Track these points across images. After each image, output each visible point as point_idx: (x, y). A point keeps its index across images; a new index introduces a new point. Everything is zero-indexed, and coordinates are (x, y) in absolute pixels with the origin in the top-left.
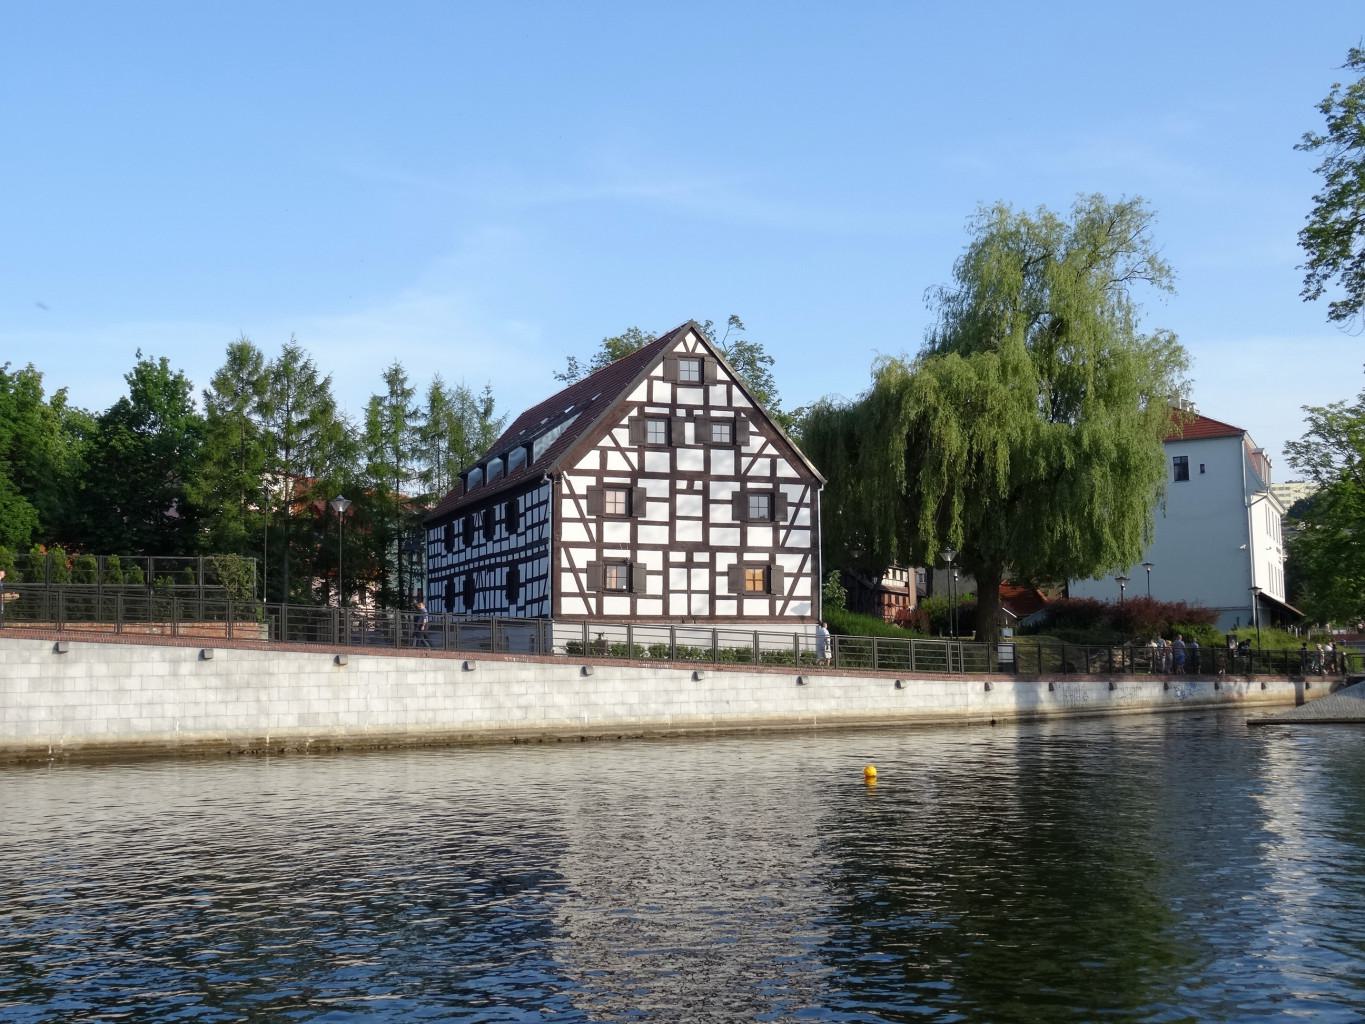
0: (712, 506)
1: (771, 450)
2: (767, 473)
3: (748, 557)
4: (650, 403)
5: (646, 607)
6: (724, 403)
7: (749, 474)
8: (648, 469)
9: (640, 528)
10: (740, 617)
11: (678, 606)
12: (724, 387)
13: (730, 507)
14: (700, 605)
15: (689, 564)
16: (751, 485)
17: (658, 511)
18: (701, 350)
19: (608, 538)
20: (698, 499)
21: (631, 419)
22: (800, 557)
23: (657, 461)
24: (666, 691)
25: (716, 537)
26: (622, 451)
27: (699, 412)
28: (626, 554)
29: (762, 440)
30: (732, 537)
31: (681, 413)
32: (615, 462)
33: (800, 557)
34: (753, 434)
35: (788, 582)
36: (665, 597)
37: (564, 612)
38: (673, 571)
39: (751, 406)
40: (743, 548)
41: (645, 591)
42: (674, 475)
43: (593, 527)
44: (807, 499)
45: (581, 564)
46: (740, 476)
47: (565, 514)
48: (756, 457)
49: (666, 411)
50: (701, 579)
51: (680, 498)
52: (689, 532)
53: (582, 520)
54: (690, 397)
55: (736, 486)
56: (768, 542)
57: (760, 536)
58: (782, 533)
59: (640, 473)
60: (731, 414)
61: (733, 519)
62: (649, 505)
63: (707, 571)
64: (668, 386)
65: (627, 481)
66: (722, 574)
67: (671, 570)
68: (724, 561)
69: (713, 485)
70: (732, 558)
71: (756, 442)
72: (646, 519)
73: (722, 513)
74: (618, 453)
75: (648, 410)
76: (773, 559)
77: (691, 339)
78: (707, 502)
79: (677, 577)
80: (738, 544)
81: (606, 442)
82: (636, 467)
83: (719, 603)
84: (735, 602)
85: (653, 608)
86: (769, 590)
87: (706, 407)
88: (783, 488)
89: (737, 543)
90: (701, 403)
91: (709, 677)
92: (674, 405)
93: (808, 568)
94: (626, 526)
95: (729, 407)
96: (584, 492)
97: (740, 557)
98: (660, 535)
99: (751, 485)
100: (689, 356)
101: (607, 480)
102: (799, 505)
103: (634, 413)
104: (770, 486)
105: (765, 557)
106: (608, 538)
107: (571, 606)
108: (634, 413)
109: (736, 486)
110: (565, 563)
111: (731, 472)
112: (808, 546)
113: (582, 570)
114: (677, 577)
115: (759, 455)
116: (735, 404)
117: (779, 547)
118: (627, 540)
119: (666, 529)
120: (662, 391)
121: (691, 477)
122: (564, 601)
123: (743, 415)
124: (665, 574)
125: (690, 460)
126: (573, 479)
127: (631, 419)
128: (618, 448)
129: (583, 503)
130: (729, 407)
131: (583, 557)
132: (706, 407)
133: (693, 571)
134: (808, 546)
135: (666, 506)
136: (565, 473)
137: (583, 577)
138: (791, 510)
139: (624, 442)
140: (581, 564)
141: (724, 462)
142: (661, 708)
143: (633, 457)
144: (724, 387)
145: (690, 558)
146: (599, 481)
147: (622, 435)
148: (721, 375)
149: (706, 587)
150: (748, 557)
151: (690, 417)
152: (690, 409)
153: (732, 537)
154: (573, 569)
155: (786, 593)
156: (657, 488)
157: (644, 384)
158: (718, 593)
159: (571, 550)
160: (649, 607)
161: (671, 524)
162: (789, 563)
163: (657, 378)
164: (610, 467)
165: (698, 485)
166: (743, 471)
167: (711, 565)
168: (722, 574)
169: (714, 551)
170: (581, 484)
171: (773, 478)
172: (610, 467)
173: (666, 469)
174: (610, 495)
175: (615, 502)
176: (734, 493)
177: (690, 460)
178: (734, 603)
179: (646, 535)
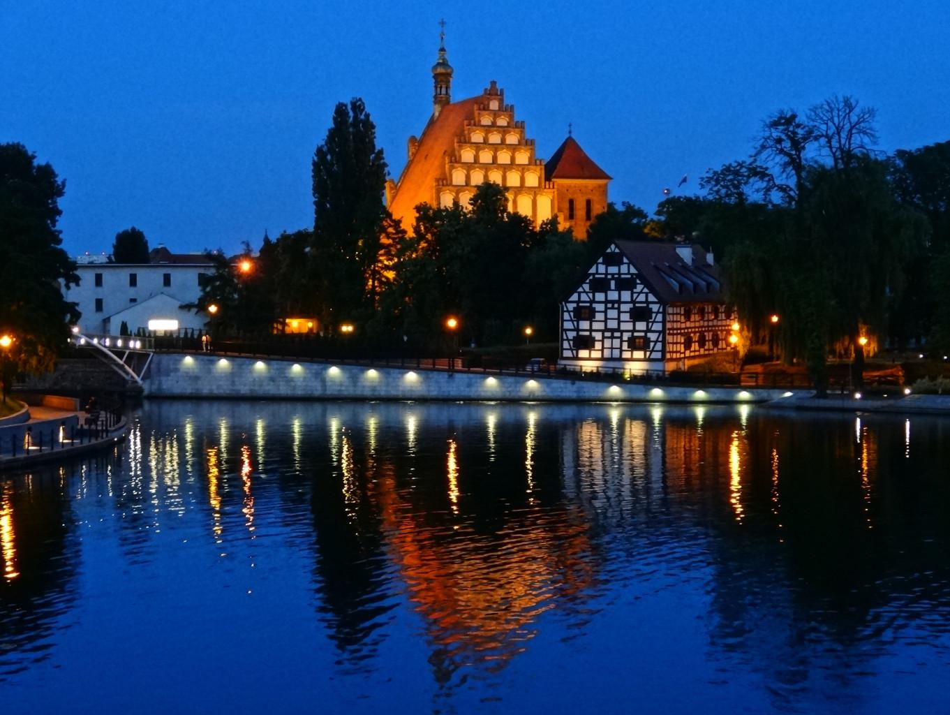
0: (622, 314)
1: (646, 290)
2: (644, 300)
3: (636, 334)
4: (597, 273)
6: (627, 272)
7: (637, 300)
8: (596, 300)
9: (593, 323)
11: (607, 353)
12: (626, 265)
13: (628, 314)
14: (616, 353)
15: (612, 337)
16: (637, 305)
17: (599, 316)
18: (617, 251)
19: (581, 328)
20: (616, 311)
21: (590, 280)
22: (657, 334)
23: (600, 296)
24: (561, 388)
25: (624, 326)
26: (587, 293)
27: (616, 276)
28: (588, 333)
29: (642, 286)
30: (629, 326)
31: (609, 277)
32: (584, 297)
33: (657, 334)
34: (639, 284)
35: (652, 344)
36: (602, 350)
37: (565, 355)
38: (605, 340)
39: (636, 272)
40: (634, 330)
41: (594, 346)
42: (606, 302)
43: (575, 323)
44: (661, 310)
45: (570, 337)
46: (633, 302)
47: (565, 318)
48: (639, 293)
49: (603, 276)
50: (616, 343)
51: (608, 310)
52: (612, 324)
53: (571, 320)
54: (613, 270)
55: (631, 305)
56: (645, 329)
57: (641, 326)
58: (650, 324)
59: (593, 301)
60: (629, 276)
61: (631, 318)
62: (597, 314)
63: (619, 340)
64: (604, 266)
65: (588, 305)
66: (625, 341)
67: (605, 340)
68: (626, 336)
69: (622, 306)
70: (630, 334)
71: (639, 288)
72: (596, 319)
73: (625, 317)
74: (584, 294)
75: (597, 276)
76: (646, 334)
77: (613, 246)
78: (619, 312)
79: (607, 343)
80: (631, 328)
81: (580, 290)
82: (591, 297)
83: (624, 353)
84: (630, 353)
87: (619, 274)
88: (651, 306)
89: (631, 328)
90: (617, 272)
91: (579, 384)
92: (606, 274)
93: (660, 339)
94: (588, 322)
95: (629, 273)
96: (572, 309)
97: (633, 334)
98: (601, 326)
99: (637, 305)
100: (613, 253)
101: (581, 304)
102: (658, 313)
103: (591, 278)
104: (645, 305)
105: (643, 334)
106: (581, 328)
107: (567, 354)
108: (591, 278)
109: (631, 305)
110: (565, 337)
111: (629, 300)
112: (661, 329)
113: (571, 340)
114: (607, 343)
115: (641, 292)
116: (631, 272)
117: (648, 330)
118: (588, 328)
119: (603, 323)
120: (602, 269)
121: (613, 302)
122: (564, 351)
123: (634, 276)
124: (603, 341)
125: (613, 295)
126: (568, 304)
127: (590, 280)
128: (585, 292)
129: (572, 314)
130: (629, 273)
131: (571, 335)
132: (619, 274)
133: (614, 340)
134: (661, 329)
135: (603, 314)
136: (564, 303)
137: (571, 342)
138: (654, 315)
139: (587, 290)
140: (570, 337)
141: (626, 296)
142: (559, 394)
143: (591, 295)
144: (626, 265)
145: (612, 334)
146: (578, 305)
147: (586, 287)
148: (625, 260)
149: (619, 346)
150: (636, 334)
151: (613, 278)
152: (613, 275)
153: (629, 326)
154: (568, 340)
155: (651, 349)
156: (600, 307)
157: (594, 267)
158: (624, 348)
159: (568, 332)
161: (605, 321)
162: (653, 337)
163: (600, 263)
164: (582, 299)
165: (616, 306)
166: (634, 298)
167: (621, 338)
168: (625, 341)
169: (622, 332)
170: (571, 306)
171: (647, 302)
172: (582, 299)
173: (603, 299)
174: (583, 311)
176: (631, 309)
177: (613, 295)
178: (630, 353)
179: (596, 326)
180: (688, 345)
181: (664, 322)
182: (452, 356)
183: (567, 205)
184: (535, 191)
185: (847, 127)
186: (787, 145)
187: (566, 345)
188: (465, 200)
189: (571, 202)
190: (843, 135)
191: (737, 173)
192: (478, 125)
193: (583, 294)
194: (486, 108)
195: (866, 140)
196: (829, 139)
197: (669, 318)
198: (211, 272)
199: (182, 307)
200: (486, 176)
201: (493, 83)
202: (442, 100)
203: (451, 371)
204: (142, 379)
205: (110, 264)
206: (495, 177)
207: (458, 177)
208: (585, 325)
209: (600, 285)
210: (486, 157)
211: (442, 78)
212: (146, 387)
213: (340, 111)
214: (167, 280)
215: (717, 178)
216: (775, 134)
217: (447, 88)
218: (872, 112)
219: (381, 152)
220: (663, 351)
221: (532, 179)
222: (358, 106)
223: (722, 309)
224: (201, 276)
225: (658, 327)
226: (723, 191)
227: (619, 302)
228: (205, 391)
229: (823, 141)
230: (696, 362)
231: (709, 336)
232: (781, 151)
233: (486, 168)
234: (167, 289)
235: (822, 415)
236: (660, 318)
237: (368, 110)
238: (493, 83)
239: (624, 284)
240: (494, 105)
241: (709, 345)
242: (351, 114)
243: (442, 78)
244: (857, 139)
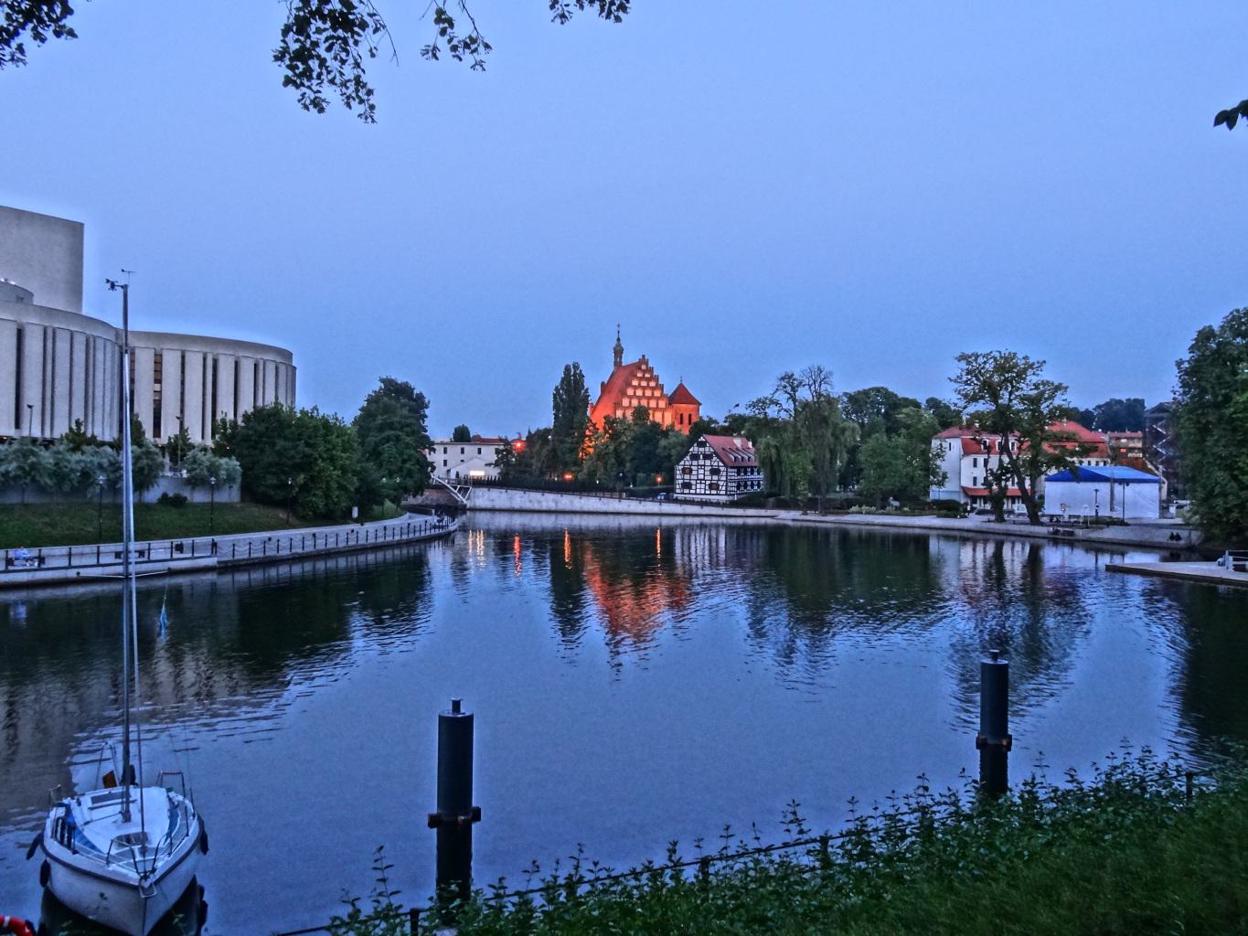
5: (692, 491)
10: (710, 494)
11: (698, 491)
14: (703, 492)
17: (694, 473)
23: (695, 463)
32: (687, 463)
52: (701, 477)
54: (702, 449)
57: (715, 478)
68: (708, 483)
71: (715, 458)
79: (698, 486)
85: (694, 491)
86: (717, 489)
107: (678, 491)
114: (698, 486)
120: (696, 449)
125: (701, 462)
131: (681, 482)
141: (708, 462)
147: (688, 458)
160: (692, 491)
170: (681, 467)
175: (687, 471)
177: (701, 462)
179: (693, 477)
180: (738, 487)
181: (727, 476)
182: (621, 491)
183: (679, 416)
184: (663, 410)
185: (819, 380)
186: (789, 389)
187: (678, 487)
188: (629, 413)
189: (682, 415)
190: (817, 385)
191: (764, 403)
192: (635, 376)
193: (687, 461)
194: (640, 368)
195: (829, 387)
196: (810, 386)
197: (729, 474)
198: (502, 447)
199: (486, 465)
200: (639, 402)
201: (643, 356)
202: (618, 364)
203: (620, 498)
204: (467, 500)
205: (451, 443)
206: (644, 403)
207: (625, 402)
208: (687, 477)
209: (695, 457)
210: (639, 393)
211: (618, 352)
212: (469, 504)
213: (567, 369)
214: (480, 452)
215: (754, 405)
216: (783, 383)
217: (621, 358)
218: (831, 373)
219: (587, 389)
220: (726, 490)
221: (662, 404)
222: (576, 367)
223: (756, 470)
224: (497, 449)
225: (724, 478)
226: (757, 411)
227: (704, 466)
228: (497, 507)
229: (807, 387)
230: (742, 496)
231: (749, 483)
232: (786, 392)
233: (639, 398)
234: (479, 456)
235: (805, 524)
236: (725, 474)
237: (581, 368)
238: (643, 356)
239: (707, 457)
240: (644, 367)
241: (749, 488)
242: (573, 370)
243: (618, 352)
244: (823, 387)
